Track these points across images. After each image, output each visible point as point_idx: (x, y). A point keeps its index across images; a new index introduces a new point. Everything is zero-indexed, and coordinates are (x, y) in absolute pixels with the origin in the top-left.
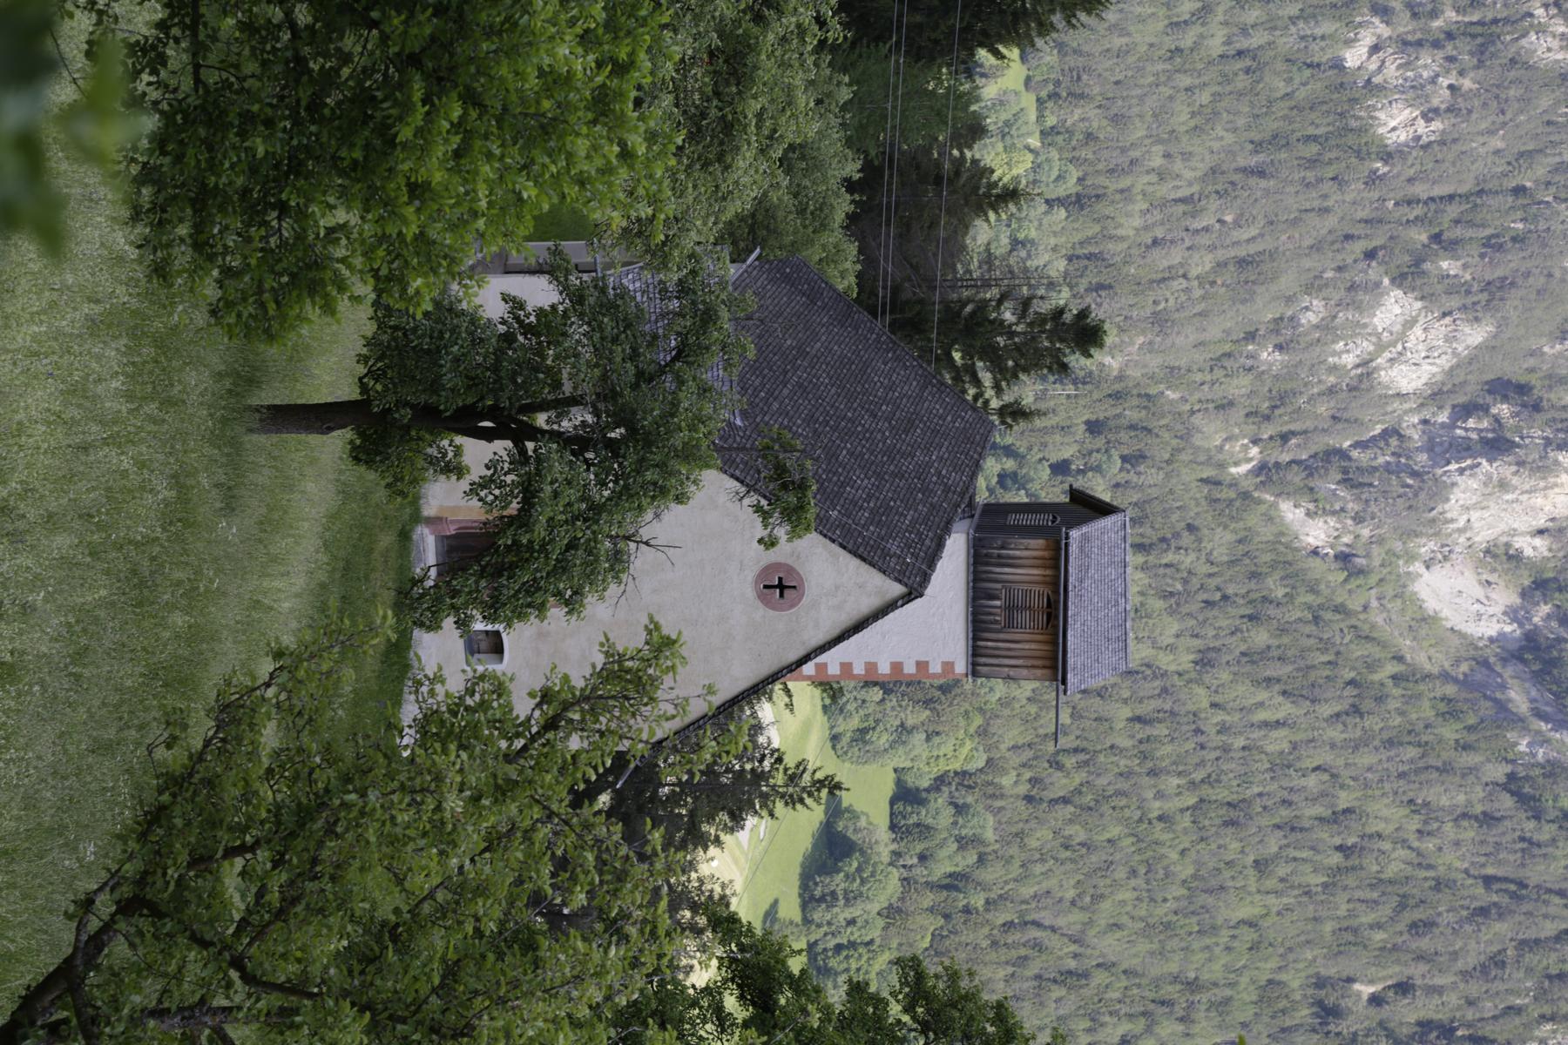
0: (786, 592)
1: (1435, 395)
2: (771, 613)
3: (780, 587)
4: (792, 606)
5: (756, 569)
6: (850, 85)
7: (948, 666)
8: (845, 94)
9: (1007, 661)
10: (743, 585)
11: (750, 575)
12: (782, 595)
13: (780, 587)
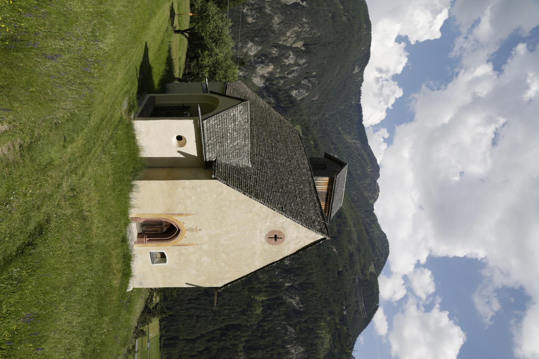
0: (278, 240)
1: (255, 56)
3: (275, 237)
4: (280, 243)
5: (266, 232)
6: (231, 22)
8: (231, 24)
10: (260, 238)
11: (264, 235)
12: (275, 240)
13: (275, 237)
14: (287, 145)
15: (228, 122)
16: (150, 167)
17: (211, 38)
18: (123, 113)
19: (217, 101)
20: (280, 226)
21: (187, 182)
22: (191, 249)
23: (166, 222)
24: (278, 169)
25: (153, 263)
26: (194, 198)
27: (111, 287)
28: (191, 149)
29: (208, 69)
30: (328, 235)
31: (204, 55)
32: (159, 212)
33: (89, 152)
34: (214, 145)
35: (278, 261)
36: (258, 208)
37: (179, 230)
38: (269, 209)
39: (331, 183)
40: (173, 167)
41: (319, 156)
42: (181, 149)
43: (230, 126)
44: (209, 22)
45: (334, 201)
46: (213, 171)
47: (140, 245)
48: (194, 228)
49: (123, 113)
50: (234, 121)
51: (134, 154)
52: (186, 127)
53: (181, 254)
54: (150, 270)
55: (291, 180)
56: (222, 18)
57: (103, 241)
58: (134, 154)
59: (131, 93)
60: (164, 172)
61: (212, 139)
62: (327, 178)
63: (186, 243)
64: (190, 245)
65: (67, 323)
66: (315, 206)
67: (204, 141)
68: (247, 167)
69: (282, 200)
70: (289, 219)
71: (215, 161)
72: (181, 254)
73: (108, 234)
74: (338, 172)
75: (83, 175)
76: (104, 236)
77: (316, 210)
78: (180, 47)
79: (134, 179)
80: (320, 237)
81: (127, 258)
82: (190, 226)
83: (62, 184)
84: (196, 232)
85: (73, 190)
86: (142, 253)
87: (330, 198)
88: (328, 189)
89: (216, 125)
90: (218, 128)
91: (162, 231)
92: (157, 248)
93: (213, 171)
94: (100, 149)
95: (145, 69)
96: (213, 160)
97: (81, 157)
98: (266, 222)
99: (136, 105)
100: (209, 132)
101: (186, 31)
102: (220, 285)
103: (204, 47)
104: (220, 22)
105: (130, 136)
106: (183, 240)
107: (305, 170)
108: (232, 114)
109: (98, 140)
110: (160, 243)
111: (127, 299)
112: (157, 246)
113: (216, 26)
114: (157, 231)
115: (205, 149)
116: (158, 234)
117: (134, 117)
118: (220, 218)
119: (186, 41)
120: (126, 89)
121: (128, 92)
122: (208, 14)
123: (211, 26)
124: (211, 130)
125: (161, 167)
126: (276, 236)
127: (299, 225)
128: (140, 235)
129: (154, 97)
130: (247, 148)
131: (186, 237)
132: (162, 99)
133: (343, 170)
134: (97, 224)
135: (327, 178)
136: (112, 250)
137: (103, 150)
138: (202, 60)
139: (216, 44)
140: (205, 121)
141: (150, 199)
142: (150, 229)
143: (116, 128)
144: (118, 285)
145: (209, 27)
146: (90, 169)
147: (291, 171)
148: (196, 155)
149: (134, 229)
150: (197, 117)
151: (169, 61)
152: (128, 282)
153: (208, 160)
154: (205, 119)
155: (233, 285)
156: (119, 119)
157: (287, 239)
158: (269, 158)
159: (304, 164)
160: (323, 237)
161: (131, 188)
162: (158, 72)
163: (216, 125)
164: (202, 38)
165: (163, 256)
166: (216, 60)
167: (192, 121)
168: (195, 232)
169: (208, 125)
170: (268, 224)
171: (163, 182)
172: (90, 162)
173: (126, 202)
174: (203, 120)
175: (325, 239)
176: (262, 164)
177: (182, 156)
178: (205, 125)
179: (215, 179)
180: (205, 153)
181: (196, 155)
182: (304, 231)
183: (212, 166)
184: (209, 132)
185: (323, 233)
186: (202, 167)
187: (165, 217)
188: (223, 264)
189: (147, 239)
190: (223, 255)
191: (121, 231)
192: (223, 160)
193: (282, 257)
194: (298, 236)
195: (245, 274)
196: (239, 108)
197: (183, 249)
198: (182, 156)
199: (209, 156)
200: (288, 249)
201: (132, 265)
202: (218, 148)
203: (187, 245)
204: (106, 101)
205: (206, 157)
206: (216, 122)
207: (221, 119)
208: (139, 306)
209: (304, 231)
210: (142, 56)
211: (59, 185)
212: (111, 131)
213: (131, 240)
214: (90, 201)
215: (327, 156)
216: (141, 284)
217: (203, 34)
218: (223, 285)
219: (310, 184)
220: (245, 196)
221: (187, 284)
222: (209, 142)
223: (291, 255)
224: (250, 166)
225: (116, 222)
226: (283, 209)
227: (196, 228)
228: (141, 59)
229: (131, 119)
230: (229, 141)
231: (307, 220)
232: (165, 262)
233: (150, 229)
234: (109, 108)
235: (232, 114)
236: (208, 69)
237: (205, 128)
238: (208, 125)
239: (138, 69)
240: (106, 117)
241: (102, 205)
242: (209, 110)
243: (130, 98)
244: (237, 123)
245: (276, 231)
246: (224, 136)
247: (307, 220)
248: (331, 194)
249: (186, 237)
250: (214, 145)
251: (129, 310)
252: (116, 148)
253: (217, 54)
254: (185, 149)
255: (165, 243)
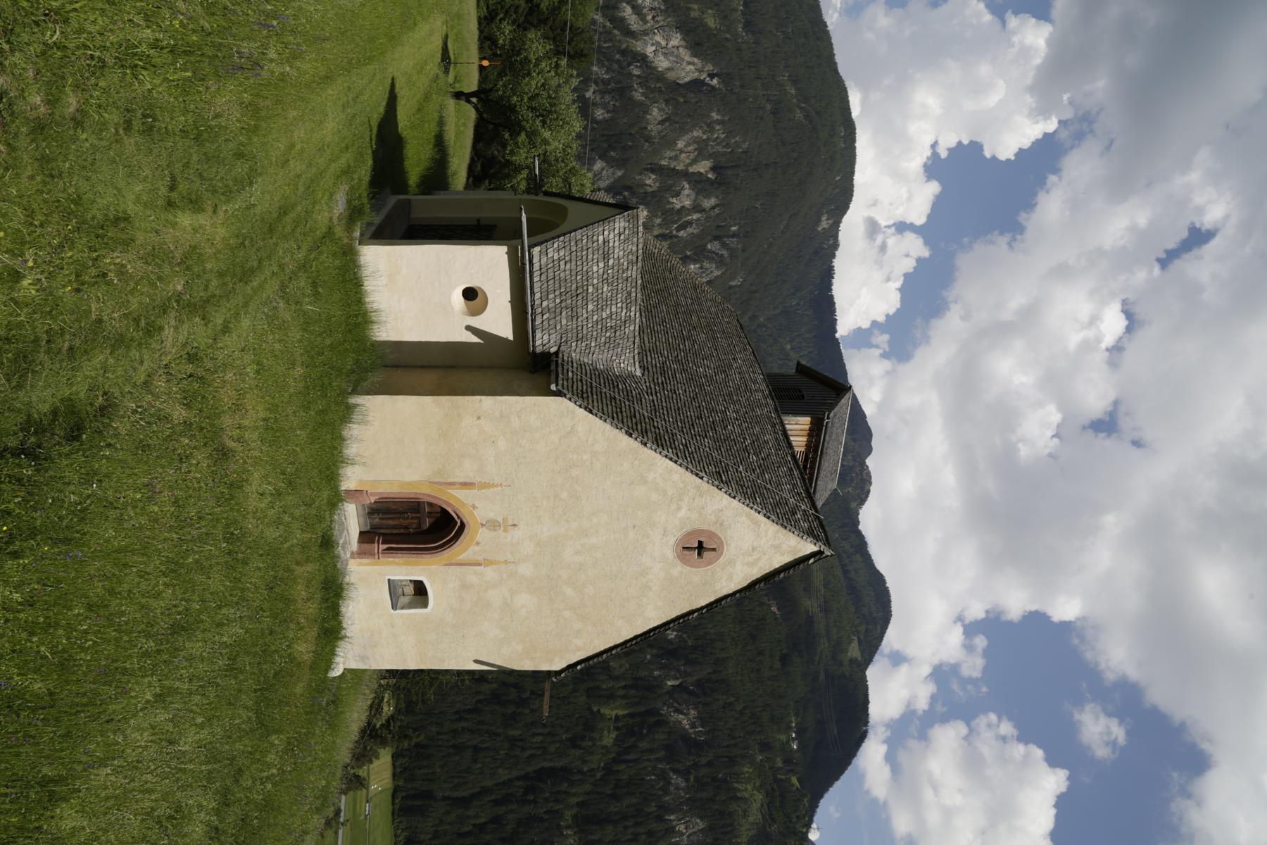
0: (706, 554)
2: (689, 568)
3: (700, 548)
4: (710, 564)
5: (679, 535)
6: (578, 76)
10: (663, 547)
12: (699, 554)
13: (700, 548)
14: (714, 337)
15: (590, 257)
16: (396, 367)
17: (533, 109)
18: (335, 221)
19: (563, 213)
20: (713, 518)
21: (487, 402)
22: (490, 573)
23: (430, 505)
24: (701, 386)
25: (394, 607)
26: (502, 443)
27: (292, 659)
28: (498, 320)
29: (525, 173)
30: (827, 543)
31: (517, 143)
32: (415, 478)
33: (246, 275)
34: (555, 312)
35: (702, 608)
36: (660, 470)
37: (463, 526)
38: (688, 474)
39: (816, 431)
40: (453, 367)
41: (783, 371)
42: (477, 322)
43: (595, 268)
44: (529, 74)
45: (822, 474)
46: (553, 376)
47: (365, 561)
48: (500, 519)
49: (335, 221)
50: (606, 257)
51: (357, 325)
52: (488, 264)
53: (465, 586)
54: (386, 627)
55: (731, 414)
56: (557, 66)
57: (272, 533)
58: (357, 325)
59: (356, 176)
60: (431, 377)
61: (551, 296)
62: (807, 420)
63: (480, 558)
64: (488, 563)
65: (152, 743)
66: (791, 475)
67: (533, 301)
68: (632, 376)
69: (715, 454)
70: (735, 502)
71: (557, 353)
72: (465, 586)
73: (287, 518)
74: (831, 407)
75: (226, 329)
76: (278, 522)
77: (794, 485)
78: (461, 126)
79: (355, 392)
80: (809, 547)
81: (332, 591)
82: (491, 515)
83: (161, 329)
84: (505, 530)
85: (192, 358)
86: (369, 580)
87: (812, 468)
88: (808, 446)
89: (562, 263)
90: (566, 270)
91: (420, 526)
92: (405, 569)
93: (553, 376)
94: (274, 285)
95: (388, 141)
96: (553, 350)
97: (221, 274)
98: (679, 508)
99: (367, 208)
100: (544, 277)
101: (473, 94)
102: (558, 668)
103: (516, 128)
104: (549, 77)
105: (350, 281)
106: (470, 551)
107: (759, 396)
108: (601, 238)
109: (269, 258)
110: (413, 558)
111: (329, 695)
112: (406, 564)
113: (543, 85)
114: (406, 527)
115: (533, 321)
116: (409, 534)
117: (362, 235)
118: (564, 495)
119: (472, 114)
120: (343, 161)
121: (347, 172)
122: (526, 58)
123: (532, 84)
124: (551, 275)
125: (423, 367)
126: (700, 543)
127: (761, 517)
128: (365, 537)
129: (409, 201)
130: (632, 328)
131: (478, 544)
132: (428, 207)
133: (843, 401)
134: (258, 486)
135: (807, 420)
136: (298, 563)
137: (283, 287)
138: (512, 153)
139: (544, 122)
140: (536, 250)
141: (393, 445)
142: (391, 522)
143: (316, 247)
144: (307, 657)
145: (528, 84)
146: (246, 323)
147: (730, 394)
148: (511, 338)
149: (351, 520)
150: (514, 242)
151: (440, 142)
152: (333, 653)
153: (539, 350)
154: (536, 245)
155: (591, 667)
156: (324, 230)
157: (728, 552)
158: (677, 361)
159: (755, 382)
160: (815, 549)
161: (347, 412)
162: (416, 160)
163: (562, 263)
164: (512, 109)
165: (420, 590)
166: (544, 154)
167: (505, 249)
168: (501, 531)
169: (544, 260)
170: (682, 513)
171: (428, 400)
172: (246, 305)
173: (336, 448)
174: (531, 247)
175: (820, 552)
176: (663, 373)
177: (475, 339)
178: (536, 260)
179: (558, 394)
180: (534, 332)
181: (511, 338)
182: (770, 532)
183: (549, 365)
184: (544, 277)
185: (816, 538)
186: (524, 366)
187: (428, 491)
188: (567, 614)
189: (383, 547)
190: (569, 591)
191: (320, 519)
192: (575, 353)
193: (712, 599)
194: (755, 544)
195: (621, 641)
196: (617, 225)
197: (470, 574)
198: (475, 339)
199: (543, 340)
200: (730, 578)
201: (343, 609)
202: (564, 322)
203: (480, 565)
204: (296, 166)
205: (534, 341)
206: (562, 253)
207: (574, 249)
208: (355, 716)
209: (770, 532)
210: (384, 103)
211: (152, 330)
212: (304, 248)
213: (343, 548)
214: (245, 422)
215: (801, 369)
216: (363, 658)
217: (515, 98)
218: (564, 665)
219: (774, 426)
220: (631, 441)
221: (476, 661)
222: (545, 304)
223: (734, 593)
224: (639, 373)
225: (308, 492)
226: (721, 476)
227: (505, 520)
228: (382, 110)
229: (352, 239)
230: (590, 307)
231: (777, 504)
232: (425, 605)
233: (391, 522)
234: (301, 189)
235: (601, 238)
236: (525, 173)
237: (536, 267)
238: (544, 260)
239: (375, 124)
240: (293, 206)
241: (273, 432)
242: (545, 229)
243: (352, 188)
244: (611, 262)
245: (701, 531)
246: (579, 293)
247: (777, 504)
248: (814, 459)
249: (478, 544)
250: (555, 312)
251: (333, 725)
252: (316, 294)
253: (545, 142)
254: (480, 322)
255: (426, 558)
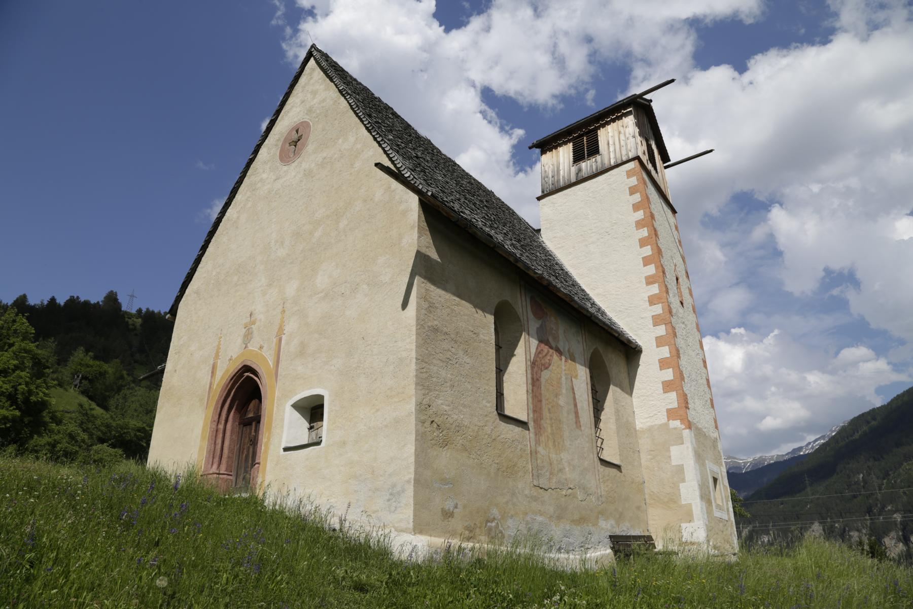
2: (312, 137)
7: (629, 174)
9: (622, 143)
25: (318, 443)
48: (244, 330)
53: (302, 352)
63: (275, 340)
64: (281, 330)
72: (302, 352)
82: (239, 341)
84: (254, 323)
98: (261, 180)
131: (261, 347)
170: (264, 176)
197: (289, 347)
203: (280, 340)
216: (394, 495)
249: (261, 347)
